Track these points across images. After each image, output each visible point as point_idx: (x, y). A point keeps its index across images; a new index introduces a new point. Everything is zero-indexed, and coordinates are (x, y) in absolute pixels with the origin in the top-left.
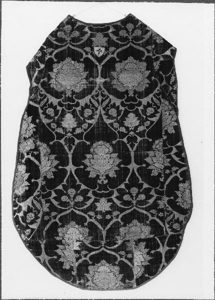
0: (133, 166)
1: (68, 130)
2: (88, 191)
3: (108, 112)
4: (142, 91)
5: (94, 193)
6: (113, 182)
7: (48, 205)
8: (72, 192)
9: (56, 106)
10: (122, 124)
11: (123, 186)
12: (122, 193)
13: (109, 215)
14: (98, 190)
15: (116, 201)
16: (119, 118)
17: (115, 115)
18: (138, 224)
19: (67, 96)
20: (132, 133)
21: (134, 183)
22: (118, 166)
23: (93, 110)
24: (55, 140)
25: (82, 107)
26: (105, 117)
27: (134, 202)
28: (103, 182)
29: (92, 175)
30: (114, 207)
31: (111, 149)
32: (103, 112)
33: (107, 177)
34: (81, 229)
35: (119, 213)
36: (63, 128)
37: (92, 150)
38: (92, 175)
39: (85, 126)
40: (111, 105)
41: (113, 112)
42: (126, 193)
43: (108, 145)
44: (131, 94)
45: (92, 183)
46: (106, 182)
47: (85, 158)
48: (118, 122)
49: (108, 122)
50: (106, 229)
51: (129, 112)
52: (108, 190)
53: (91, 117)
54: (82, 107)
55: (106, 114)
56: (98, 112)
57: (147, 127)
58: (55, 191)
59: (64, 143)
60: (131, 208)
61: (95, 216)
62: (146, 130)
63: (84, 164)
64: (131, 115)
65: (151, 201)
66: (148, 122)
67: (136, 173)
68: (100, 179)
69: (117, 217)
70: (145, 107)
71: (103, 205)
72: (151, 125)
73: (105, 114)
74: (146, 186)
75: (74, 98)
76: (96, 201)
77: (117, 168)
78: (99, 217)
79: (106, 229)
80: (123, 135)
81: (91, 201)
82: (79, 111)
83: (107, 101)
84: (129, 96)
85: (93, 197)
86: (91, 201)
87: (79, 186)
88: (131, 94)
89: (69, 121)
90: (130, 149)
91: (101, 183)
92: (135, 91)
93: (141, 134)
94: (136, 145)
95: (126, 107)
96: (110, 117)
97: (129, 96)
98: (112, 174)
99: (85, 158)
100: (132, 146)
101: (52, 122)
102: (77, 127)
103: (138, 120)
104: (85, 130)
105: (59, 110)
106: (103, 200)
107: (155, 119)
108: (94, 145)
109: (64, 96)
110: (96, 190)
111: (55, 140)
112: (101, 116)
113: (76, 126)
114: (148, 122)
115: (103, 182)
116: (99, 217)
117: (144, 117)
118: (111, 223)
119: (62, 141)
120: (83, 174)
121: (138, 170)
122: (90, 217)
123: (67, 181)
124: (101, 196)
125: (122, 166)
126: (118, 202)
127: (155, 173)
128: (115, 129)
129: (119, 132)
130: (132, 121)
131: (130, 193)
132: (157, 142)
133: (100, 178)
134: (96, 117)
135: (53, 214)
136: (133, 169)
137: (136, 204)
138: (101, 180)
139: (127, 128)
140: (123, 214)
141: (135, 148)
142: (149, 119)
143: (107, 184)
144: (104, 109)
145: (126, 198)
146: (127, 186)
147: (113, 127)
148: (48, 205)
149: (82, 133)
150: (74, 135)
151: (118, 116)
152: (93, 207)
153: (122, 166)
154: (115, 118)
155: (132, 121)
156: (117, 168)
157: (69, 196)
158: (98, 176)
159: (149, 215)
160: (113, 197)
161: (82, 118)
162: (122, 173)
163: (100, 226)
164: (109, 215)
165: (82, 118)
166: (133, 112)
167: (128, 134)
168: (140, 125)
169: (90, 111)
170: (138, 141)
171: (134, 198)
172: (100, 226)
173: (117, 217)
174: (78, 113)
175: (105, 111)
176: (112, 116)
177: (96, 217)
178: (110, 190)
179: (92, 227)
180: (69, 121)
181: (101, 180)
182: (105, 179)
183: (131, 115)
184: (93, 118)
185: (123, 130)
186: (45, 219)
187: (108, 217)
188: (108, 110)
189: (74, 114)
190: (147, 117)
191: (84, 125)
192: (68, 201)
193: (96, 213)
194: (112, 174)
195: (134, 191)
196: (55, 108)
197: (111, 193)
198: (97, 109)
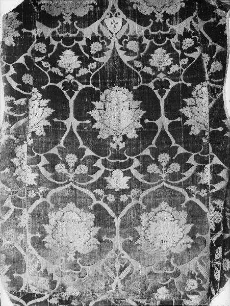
0: (163, 122)
1: (67, 71)
2: (97, 159)
3: (125, 46)
4: (176, 13)
5: (105, 163)
6: (133, 146)
7: (36, 175)
8: (71, 159)
9: (49, 39)
10: (147, 64)
11: (147, 152)
12: (146, 161)
13: (125, 195)
14: (111, 158)
15: (135, 173)
16: (142, 54)
17: (137, 50)
18: (170, 209)
19: (65, 23)
21: (164, 145)
22: (142, 120)
23: (103, 43)
24: (49, 84)
25: (88, 40)
26: (121, 54)
27: (164, 176)
28: (118, 146)
29: (103, 135)
30: (133, 183)
31: (131, 96)
32: (118, 46)
33: (125, 137)
34: (83, 214)
35: (140, 191)
36: (60, 68)
37: (102, 97)
38: (103, 135)
39: (93, 65)
41: (133, 46)
42: (152, 162)
43: (126, 91)
44: (159, 18)
45: (101, 147)
46: (122, 146)
47: (93, 107)
49: (126, 59)
50: (122, 215)
51: (157, 47)
52: (126, 158)
53: (100, 54)
54: (88, 40)
56: (111, 46)
57: (184, 66)
58: (46, 156)
59: (61, 88)
60: (159, 184)
61: (104, 196)
62: (182, 71)
63: (91, 118)
64: (160, 51)
65: (188, 174)
66: (185, 61)
68: (114, 142)
69: (137, 197)
70: (181, 38)
71: (118, 180)
72: (189, 63)
73: (121, 49)
74: (181, 150)
75: (75, 24)
76: (107, 174)
78: (111, 198)
79: (122, 215)
80: (147, 77)
81: (99, 174)
82: (84, 46)
84: (157, 21)
85: (103, 169)
86: (99, 174)
87: (83, 150)
88: (159, 18)
89: (69, 60)
90: (159, 96)
91: (115, 148)
92: (165, 13)
93: (175, 76)
95: (153, 40)
96: (128, 52)
97: (157, 21)
98: (132, 135)
99: (93, 107)
100: (162, 94)
101: (44, 60)
102: (81, 67)
103: (170, 57)
104: (93, 70)
105: (53, 46)
106: (118, 173)
107: (195, 55)
108: (107, 91)
109: (60, 23)
110: (107, 158)
111: (49, 84)
112: (114, 51)
113: (79, 66)
114: (185, 61)
115: (118, 146)
116: (111, 198)
117: (179, 52)
118: (129, 206)
119: (60, 85)
120: (90, 135)
121: (170, 126)
122: (98, 198)
123: (65, 143)
124: (116, 166)
125: (147, 121)
126: (139, 176)
127: (195, 131)
128: (136, 68)
129: (142, 73)
130: (160, 58)
131: (158, 164)
132: (198, 87)
133: (114, 140)
134: (108, 54)
135: (42, 189)
136: (163, 126)
137: (166, 177)
138: (116, 144)
139: (154, 69)
140: (146, 192)
142: (186, 54)
143: (123, 149)
144: (120, 42)
145: (152, 168)
146: (156, 152)
147: (133, 65)
148: (36, 175)
149: (89, 74)
150: (76, 78)
152: (101, 183)
153: (147, 121)
154: (136, 53)
155: (160, 58)
157: (66, 164)
158: (112, 136)
160: (132, 168)
161: (88, 56)
162: (147, 131)
163: (111, 213)
164: (125, 195)
165: (88, 56)
166: (163, 47)
167: (155, 77)
168: (176, 62)
169: (100, 45)
170: (171, 87)
171: (163, 170)
172: (111, 213)
174: (82, 49)
175: (122, 45)
176: (132, 51)
177: (105, 198)
178: (128, 157)
179: (98, 207)
180: (69, 60)
181: (116, 144)
182: (122, 142)
183: (160, 51)
184: (104, 55)
185: (148, 70)
186: (29, 196)
187: (124, 198)
188: (126, 43)
189: (76, 50)
190: (183, 51)
191: (91, 64)
192: (65, 171)
193: (107, 192)
194: (132, 135)
195: (164, 158)
196: (47, 42)
197: (130, 162)
198: (109, 41)
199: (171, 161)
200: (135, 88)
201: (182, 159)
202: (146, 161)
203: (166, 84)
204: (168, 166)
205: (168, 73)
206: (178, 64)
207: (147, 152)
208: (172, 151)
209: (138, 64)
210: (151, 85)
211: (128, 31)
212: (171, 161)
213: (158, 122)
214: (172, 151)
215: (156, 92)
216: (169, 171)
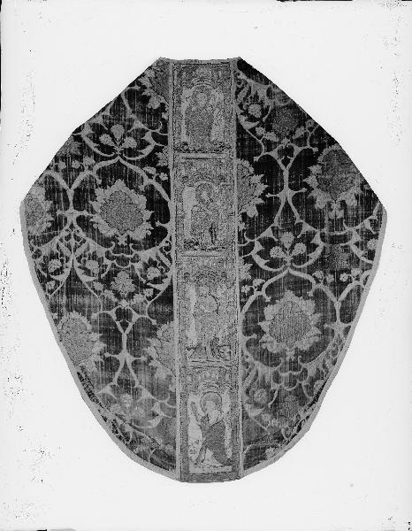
0: (286, 195)
3: (247, 111)
20: (285, 141)
22: (263, 196)
40: (251, 98)
48: (262, 124)
55: (246, 113)
67: (291, 204)
77: (261, 201)
80: (270, 145)
83: (246, 89)
90: (282, 167)
93: (300, 141)
94: (292, 159)
98: (252, 212)
141: (290, 165)
151: (263, 116)
153: (269, 195)
156: (261, 201)
159: (314, 282)
168: (299, 126)
173: (260, 289)
197: (252, 245)
199: (296, 241)
200: (256, 159)
201: (307, 239)
202: (268, 244)
203: (289, 151)
204: (292, 248)
205: (294, 138)
206: (305, 126)
207: (268, 233)
208: (296, 229)
209: (260, 131)
210: (274, 154)
211: (250, 91)
212: (296, 241)
213: (281, 195)
214: (296, 229)
215: (280, 162)
216: (294, 253)
